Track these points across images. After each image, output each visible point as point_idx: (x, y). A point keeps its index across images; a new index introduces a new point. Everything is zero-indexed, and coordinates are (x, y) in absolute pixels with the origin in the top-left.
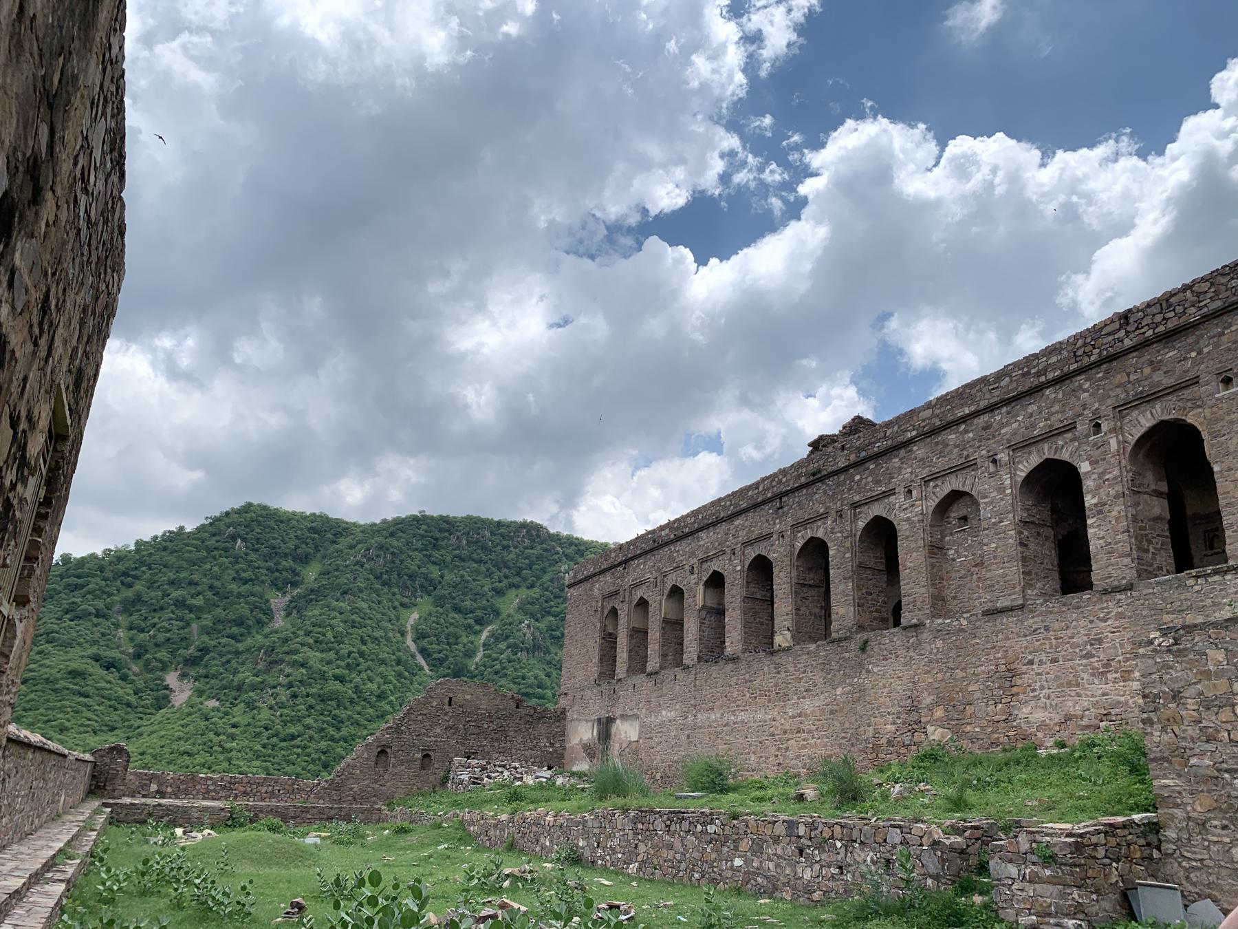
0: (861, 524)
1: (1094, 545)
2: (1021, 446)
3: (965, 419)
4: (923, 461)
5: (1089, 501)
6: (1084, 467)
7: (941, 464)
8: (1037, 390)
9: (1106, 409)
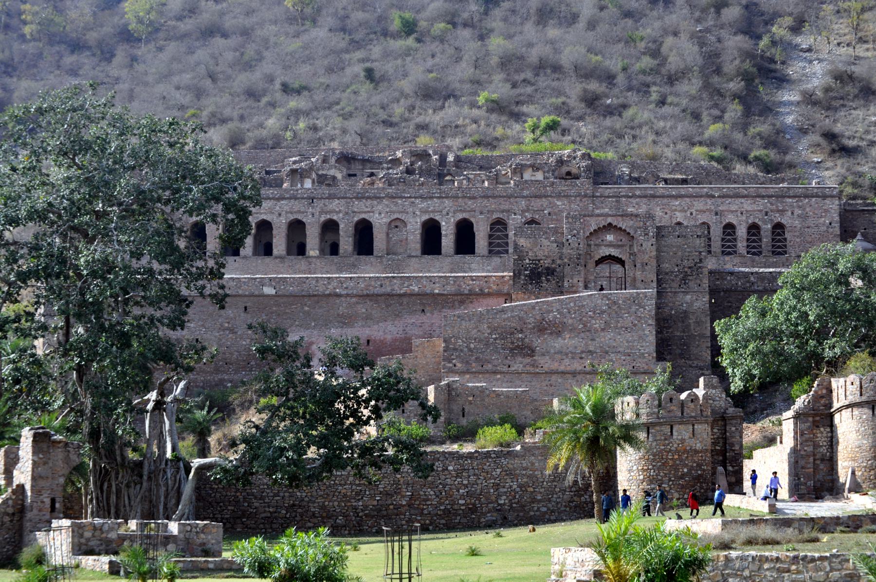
0: (356, 219)
1: (443, 244)
2: (424, 211)
3: (405, 198)
4: (387, 206)
5: (443, 233)
6: (444, 223)
7: (394, 208)
8: (431, 198)
9: (452, 210)
